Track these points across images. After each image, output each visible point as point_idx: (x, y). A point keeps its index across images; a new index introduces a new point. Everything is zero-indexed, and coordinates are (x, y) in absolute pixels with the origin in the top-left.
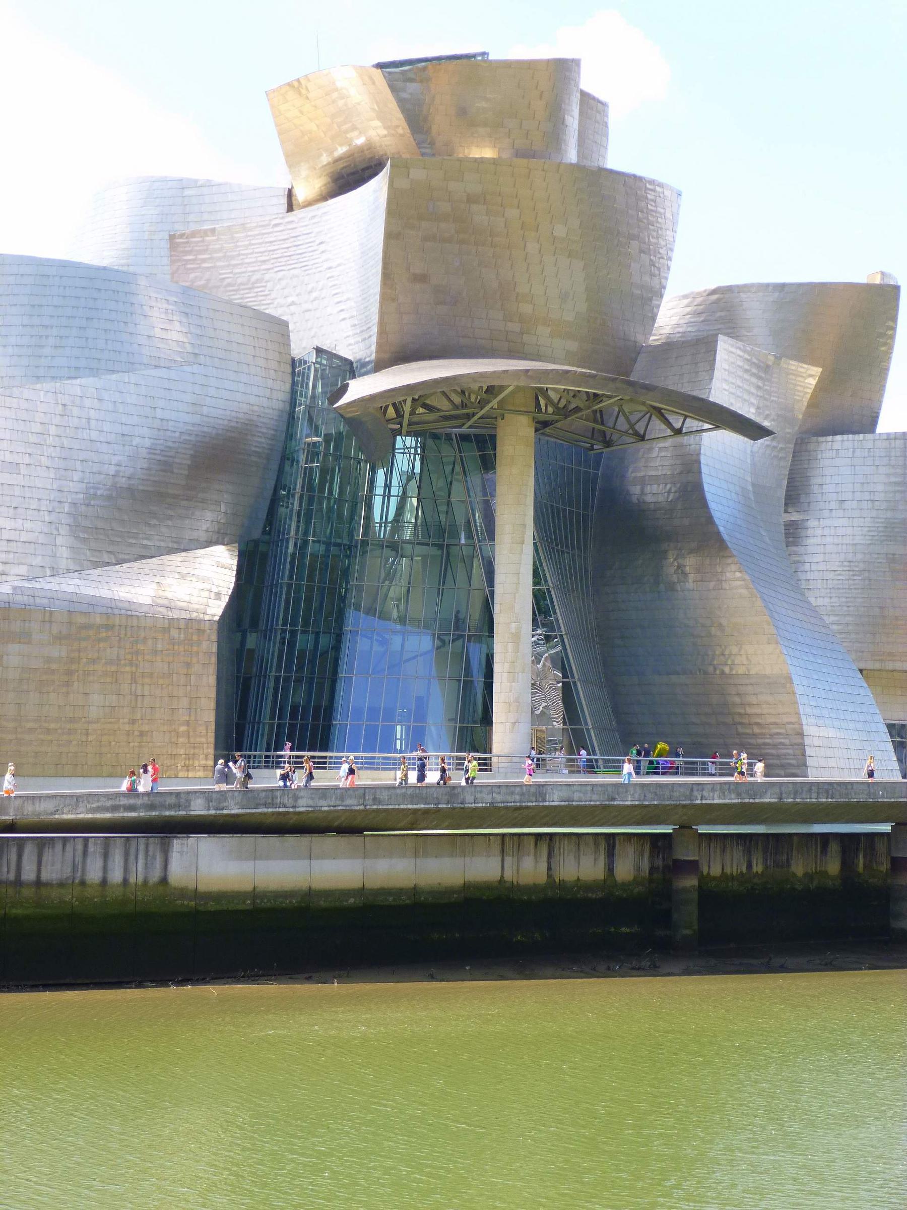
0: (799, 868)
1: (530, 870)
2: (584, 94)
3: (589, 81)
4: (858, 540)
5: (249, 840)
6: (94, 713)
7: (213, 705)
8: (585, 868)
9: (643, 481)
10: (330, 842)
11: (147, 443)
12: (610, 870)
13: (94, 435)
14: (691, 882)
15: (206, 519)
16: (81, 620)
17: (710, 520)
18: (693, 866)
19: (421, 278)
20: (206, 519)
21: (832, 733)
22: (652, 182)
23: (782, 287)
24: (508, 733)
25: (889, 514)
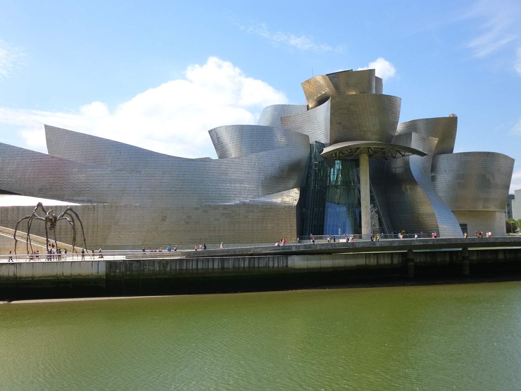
0: (439, 259)
1: (373, 262)
2: (376, 77)
3: (377, 74)
4: (450, 179)
5: (306, 256)
6: (269, 228)
7: (296, 225)
8: (386, 261)
9: (395, 168)
10: (324, 256)
11: (278, 166)
12: (392, 261)
13: (266, 165)
14: (412, 264)
15: (292, 182)
16: (265, 207)
17: (413, 176)
18: (412, 260)
19: (340, 123)
20: (292, 182)
21: (445, 227)
22: (394, 97)
23: (428, 119)
24: (365, 230)
25: (458, 173)
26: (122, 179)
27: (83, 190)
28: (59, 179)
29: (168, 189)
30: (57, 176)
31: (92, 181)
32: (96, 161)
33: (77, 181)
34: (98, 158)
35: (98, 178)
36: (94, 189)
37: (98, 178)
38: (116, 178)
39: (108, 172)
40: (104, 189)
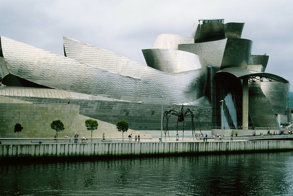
25: (271, 90)
26: (130, 83)
27: (105, 90)
28: (86, 80)
29: (156, 92)
30: (85, 77)
31: (111, 83)
32: (110, 68)
33: (100, 82)
34: (111, 66)
35: (115, 81)
36: (112, 89)
37: (115, 81)
38: (127, 82)
39: (121, 78)
40: (119, 90)
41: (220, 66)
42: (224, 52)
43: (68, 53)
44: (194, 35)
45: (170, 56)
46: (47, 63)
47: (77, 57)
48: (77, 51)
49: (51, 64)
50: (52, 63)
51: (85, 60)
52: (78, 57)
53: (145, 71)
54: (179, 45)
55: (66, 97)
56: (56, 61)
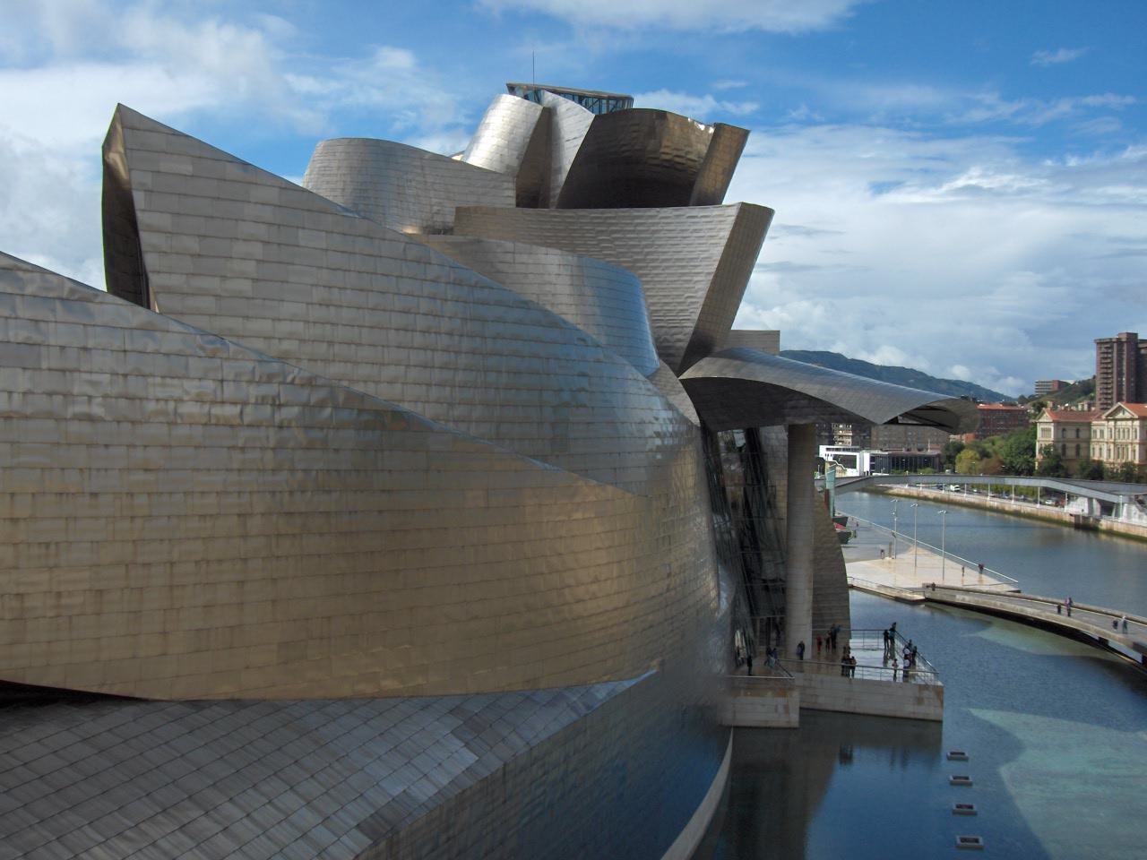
41: (688, 338)
42: (713, 269)
43: (175, 281)
44: (515, 163)
45: (548, 288)
46: (49, 415)
47: (255, 326)
48: (250, 267)
49: (90, 418)
50: (97, 410)
51: (326, 361)
52: (265, 326)
53: (658, 435)
54: (458, 210)
55: (361, 812)
56: (134, 386)
